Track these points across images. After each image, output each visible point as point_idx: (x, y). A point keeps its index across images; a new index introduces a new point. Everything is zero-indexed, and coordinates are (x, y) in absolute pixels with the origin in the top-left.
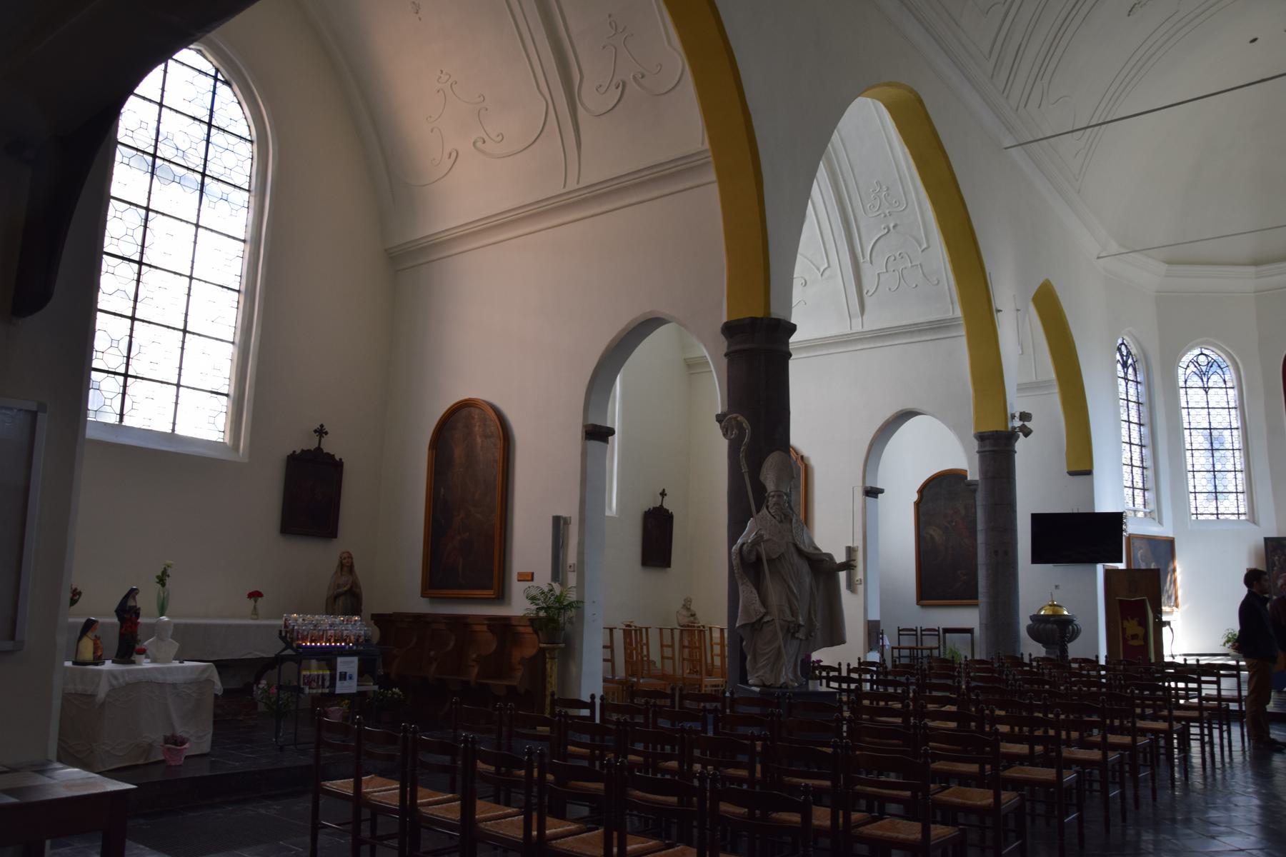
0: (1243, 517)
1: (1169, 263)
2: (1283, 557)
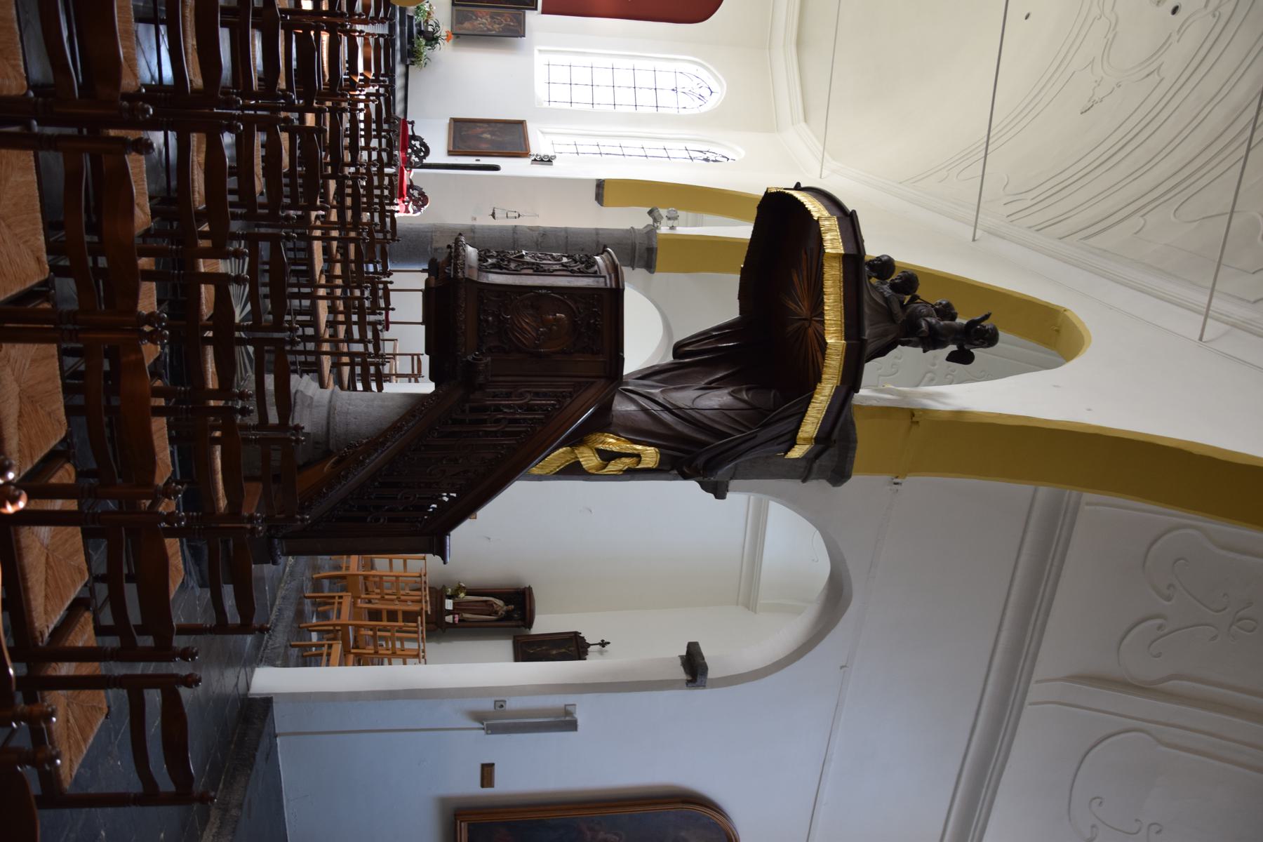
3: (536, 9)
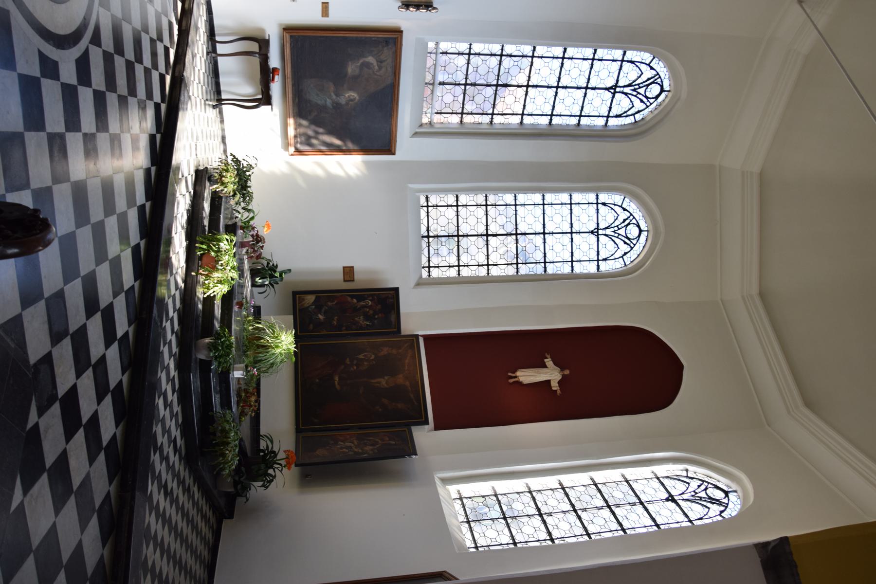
0: (425, 274)
1: (761, 175)
2: (371, 312)
3: (426, 422)
